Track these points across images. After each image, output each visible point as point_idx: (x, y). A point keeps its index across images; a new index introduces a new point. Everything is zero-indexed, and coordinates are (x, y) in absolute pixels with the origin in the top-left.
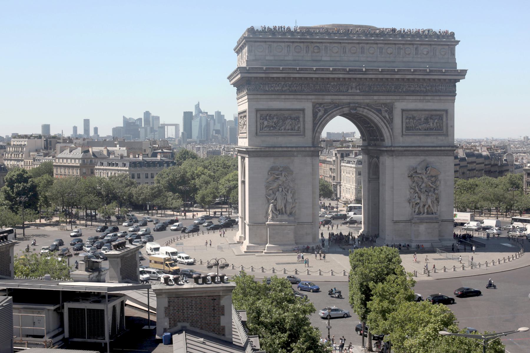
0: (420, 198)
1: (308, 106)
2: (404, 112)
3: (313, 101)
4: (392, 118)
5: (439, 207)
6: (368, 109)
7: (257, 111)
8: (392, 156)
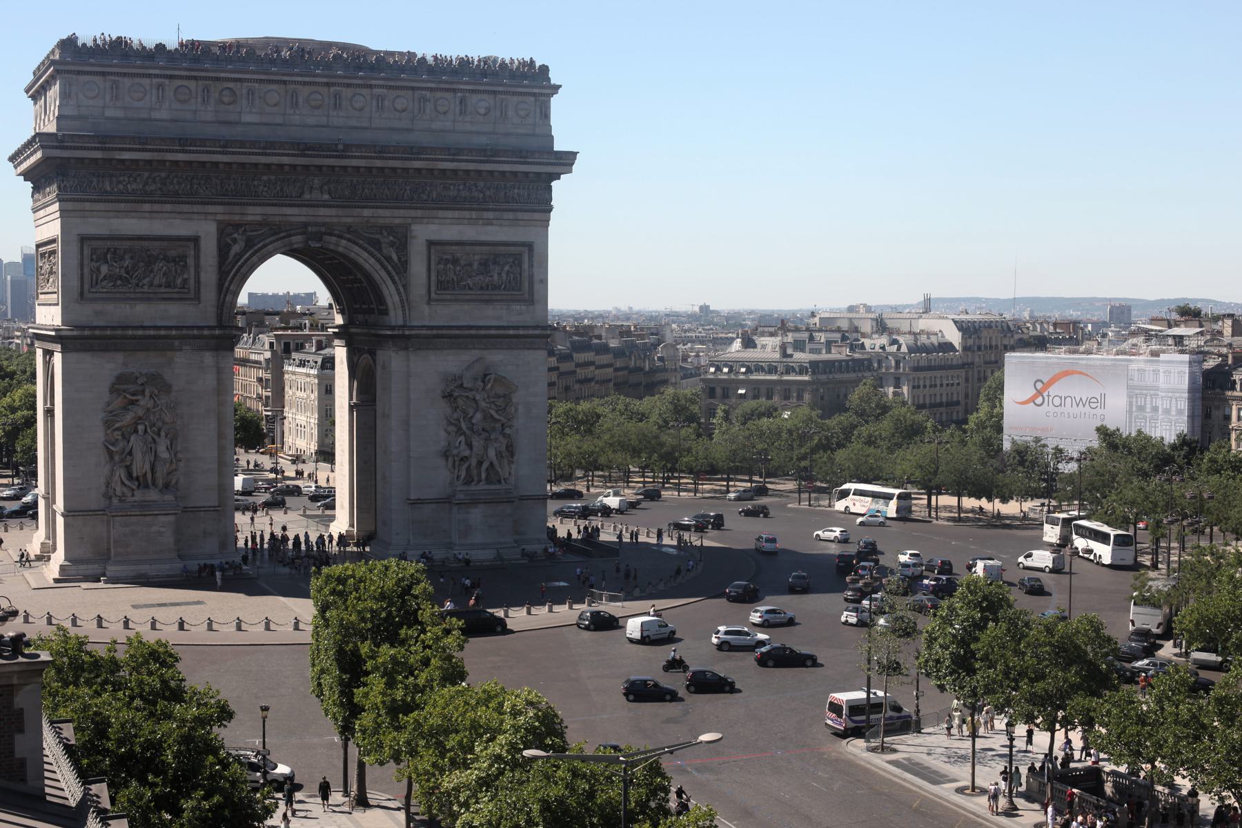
0: (470, 446)
1: (207, 231)
3: (219, 217)
4: (406, 262)
5: (513, 466)
6: (349, 240)
7: (83, 239)
8: (406, 349)
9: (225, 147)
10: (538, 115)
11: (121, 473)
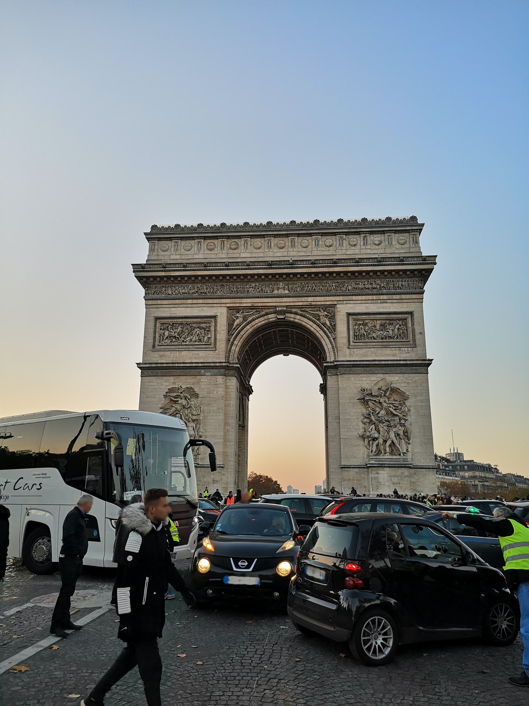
0: (379, 432)
1: (221, 313)
2: (351, 318)
3: (228, 305)
6: (301, 315)
7: (157, 319)
10: (411, 242)
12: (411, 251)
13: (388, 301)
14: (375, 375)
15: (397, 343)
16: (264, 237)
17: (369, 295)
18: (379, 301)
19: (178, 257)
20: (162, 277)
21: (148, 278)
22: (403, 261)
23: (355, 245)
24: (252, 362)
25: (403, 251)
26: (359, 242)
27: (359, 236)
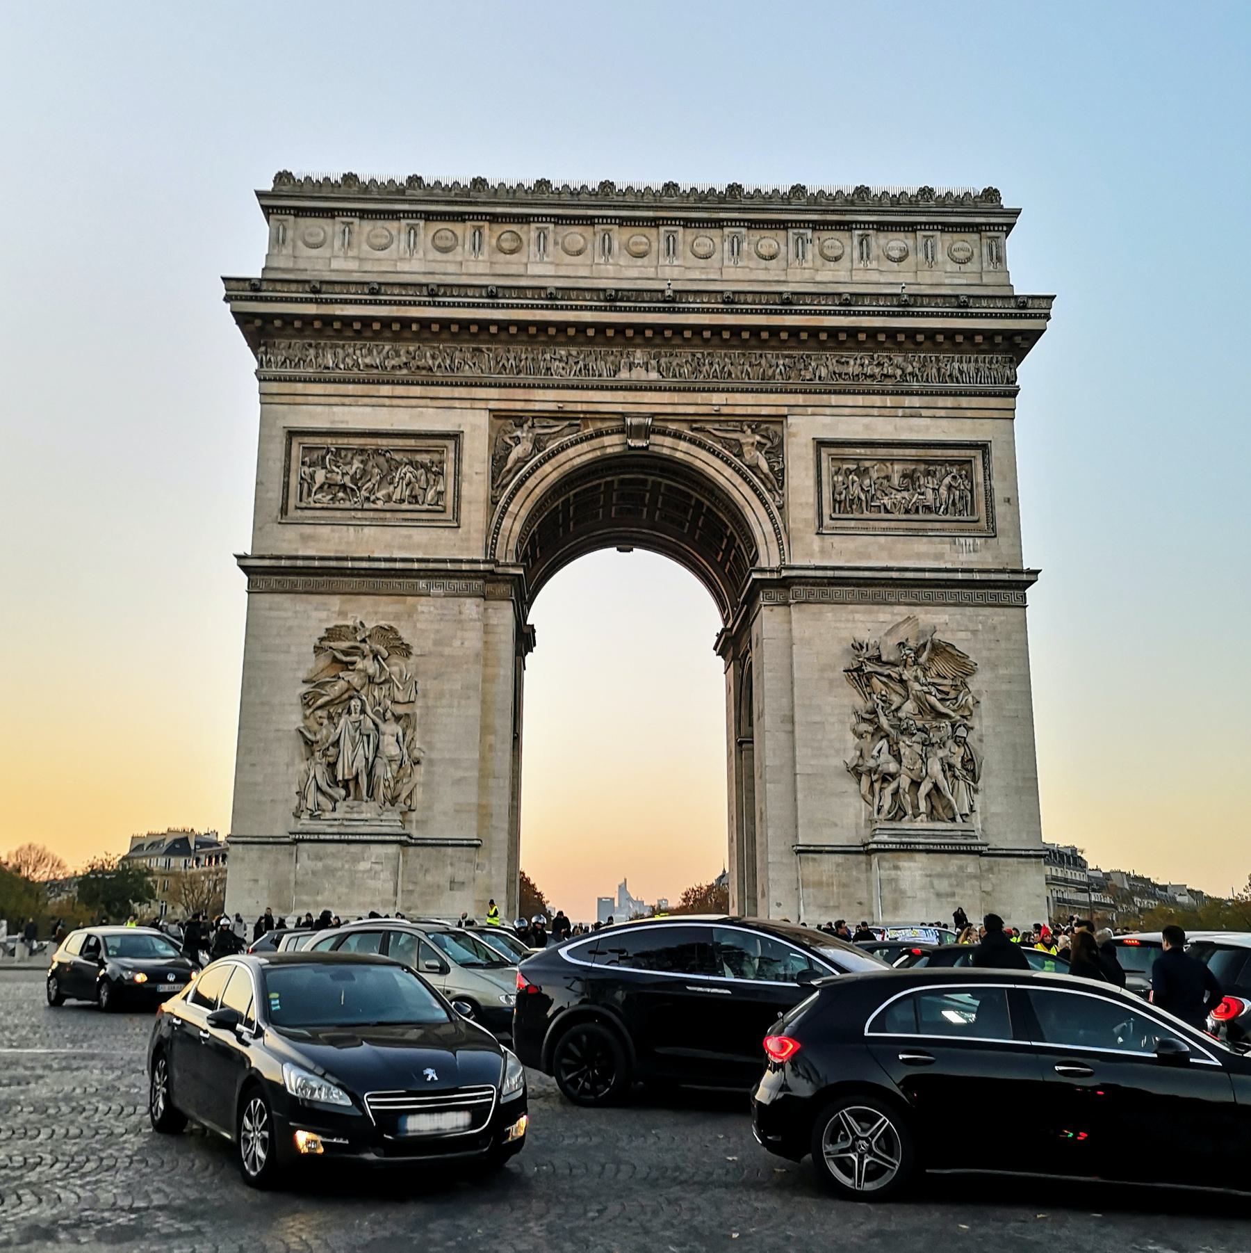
0: (898, 758)
2: (825, 452)
3: (492, 405)
6: (692, 441)
7: (292, 434)
8: (786, 604)
9: (496, 297)
11: (320, 772)
12: (985, 280)
13: (924, 412)
14: (888, 608)
15: (946, 525)
16: (593, 224)
17: (874, 393)
18: (900, 412)
19: (353, 265)
20: (307, 320)
21: (268, 318)
22: (967, 307)
23: (837, 259)
24: (538, 565)
25: (964, 282)
26: (848, 250)
27: (847, 234)
